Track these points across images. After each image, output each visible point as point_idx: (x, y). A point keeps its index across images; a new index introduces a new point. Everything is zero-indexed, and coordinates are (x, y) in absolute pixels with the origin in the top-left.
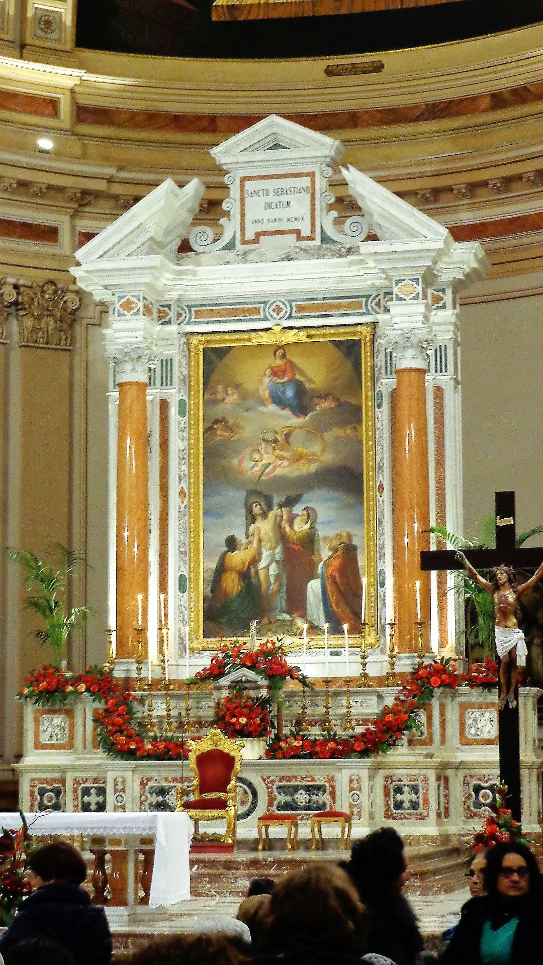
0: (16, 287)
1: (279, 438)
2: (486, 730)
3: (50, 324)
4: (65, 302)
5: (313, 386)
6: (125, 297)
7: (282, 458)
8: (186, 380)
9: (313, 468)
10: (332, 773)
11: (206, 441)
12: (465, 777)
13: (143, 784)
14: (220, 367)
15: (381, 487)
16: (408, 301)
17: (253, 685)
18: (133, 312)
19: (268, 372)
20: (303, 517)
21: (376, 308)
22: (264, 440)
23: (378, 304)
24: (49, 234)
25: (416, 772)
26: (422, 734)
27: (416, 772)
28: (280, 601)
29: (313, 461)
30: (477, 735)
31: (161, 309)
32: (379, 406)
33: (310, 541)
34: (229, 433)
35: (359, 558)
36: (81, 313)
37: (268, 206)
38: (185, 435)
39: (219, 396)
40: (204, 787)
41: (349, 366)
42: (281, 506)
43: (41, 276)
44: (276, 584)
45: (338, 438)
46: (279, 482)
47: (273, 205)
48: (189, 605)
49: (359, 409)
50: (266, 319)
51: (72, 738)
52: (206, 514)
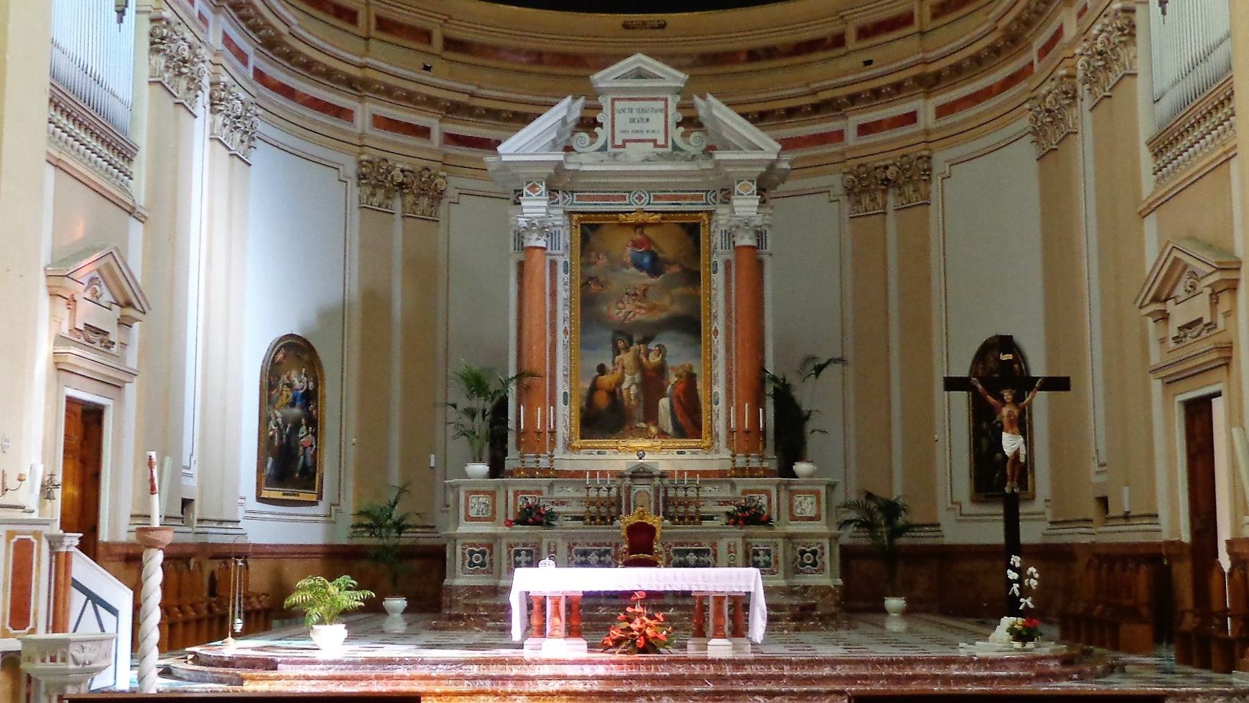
0: (402, 171)
2: (808, 510)
4: (436, 184)
5: (664, 256)
7: (640, 307)
9: (663, 315)
10: (714, 540)
13: (570, 548)
15: (716, 331)
17: (648, 474)
18: (537, 194)
19: (630, 243)
23: (715, 197)
24: (424, 132)
25: (769, 540)
27: (769, 540)
28: (639, 413)
33: (661, 370)
35: (698, 383)
36: (446, 194)
37: (632, 121)
38: (568, 287)
39: (592, 260)
40: (632, 550)
42: (639, 343)
46: (638, 325)
47: (636, 121)
48: (570, 414)
49: (698, 273)
51: (494, 512)
52: (585, 345)
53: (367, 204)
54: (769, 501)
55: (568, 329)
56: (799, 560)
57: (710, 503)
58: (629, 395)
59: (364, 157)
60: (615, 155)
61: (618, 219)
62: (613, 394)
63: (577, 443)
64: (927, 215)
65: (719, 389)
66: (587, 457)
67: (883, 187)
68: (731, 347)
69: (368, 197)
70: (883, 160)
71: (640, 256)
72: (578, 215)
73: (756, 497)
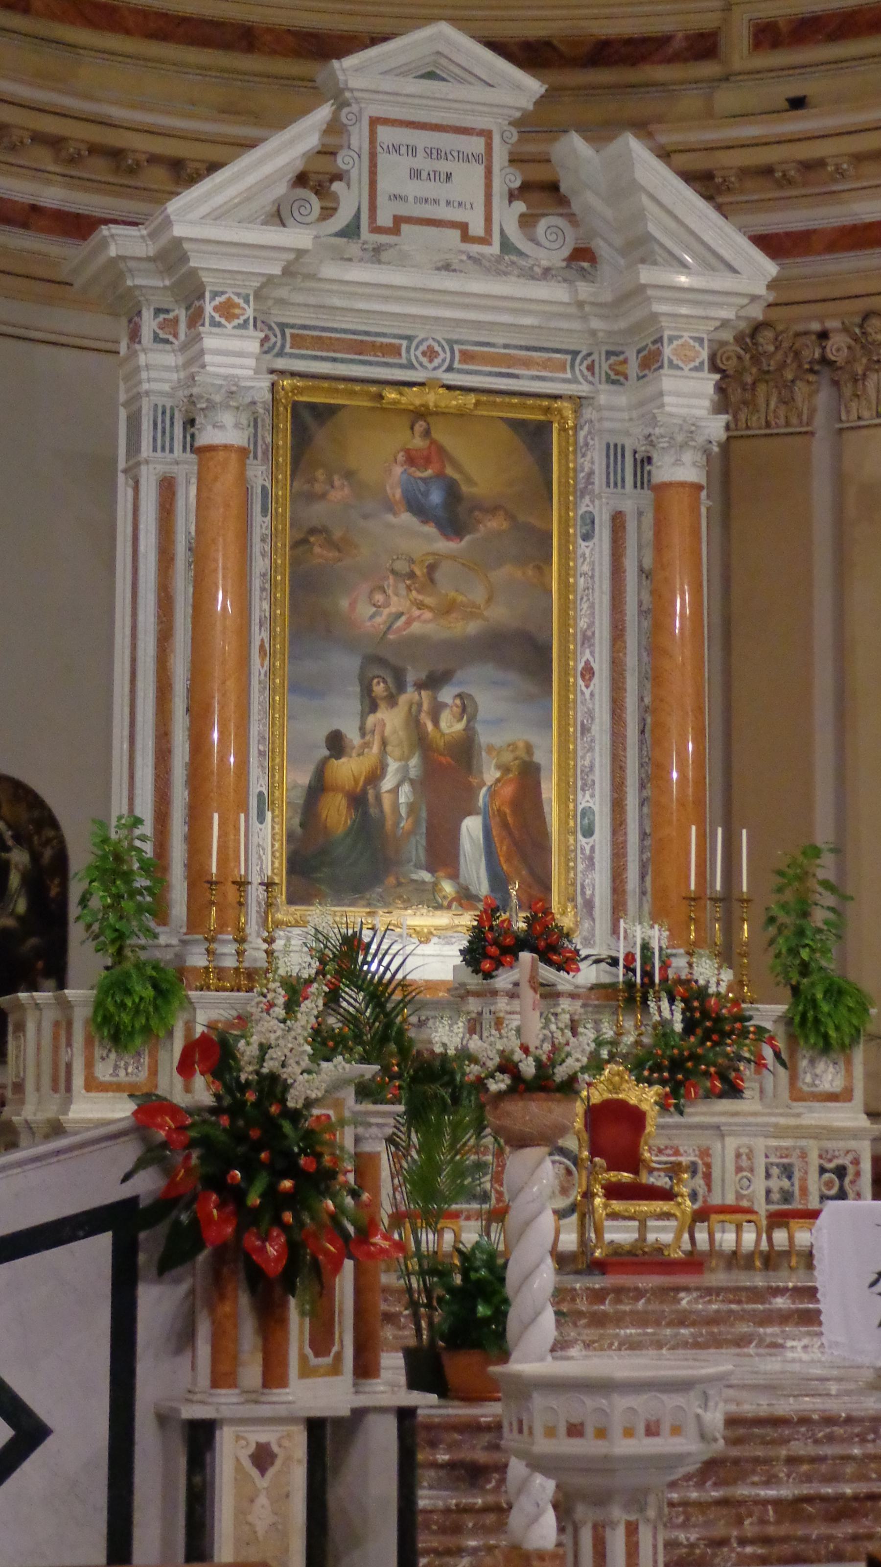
1: (418, 572)
5: (474, 490)
6: (223, 293)
7: (421, 606)
9: (472, 627)
10: (704, 1142)
11: (295, 562)
14: (321, 437)
16: (686, 372)
18: (236, 322)
19: (401, 457)
20: (455, 709)
22: (393, 571)
23: (591, 368)
29: (472, 616)
34: (332, 554)
37: (416, 174)
39: (318, 488)
42: (420, 686)
44: (410, 820)
47: (424, 175)
50: (410, 366)
58: (396, 805)
60: (378, 250)
61: (381, 397)
70: (821, 319)
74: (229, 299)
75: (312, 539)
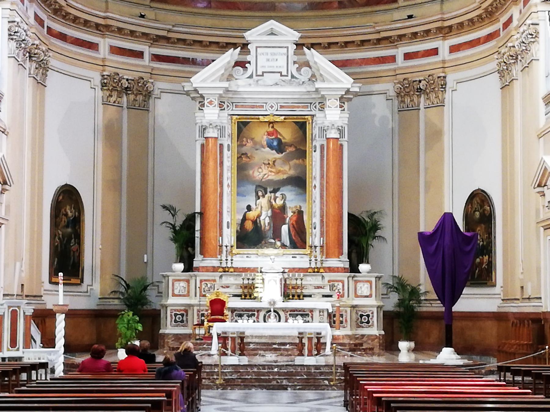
1: (270, 163)
3: (140, 98)
4: (147, 87)
7: (271, 172)
8: (231, 136)
9: (285, 177)
12: (356, 311)
14: (245, 130)
15: (315, 186)
19: (266, 134)
21: (315, 109)
23: (315, 107)
24: (139, 55)
26: (340, 293)
28: (270, 234)
29: (285, 173)
30: (361, 293)
31: (221, 103)
32: (315, 151)
33: (283, 208)
34: (249, 160)
38: (230, 159)
39: (244, 143)
41: (301, 133)
42: (271, 192)
43: (136, 75)
45: (295, 164)
46: (270, 182)
49: (306, 151)
50: (266, 110)
52: (238, 194)
53: (107, 102)
54: (343, 286)
55: (230, 184)
56: (360, 320)
57: (311, 287)
58: (265, 223)
59: (105, 73)
61: (259, 119)
62: (255, 222)
63: (235, 251)
64: (443, 111)
65: (317, 220)
66: (241, 259)
67: (418, 93)
68: (323, 196)
69: (108, 97)
71: (272, 141)
72: (237, 116)
73: (336, 284)
74: (211, 100)
75: (242, 156)
